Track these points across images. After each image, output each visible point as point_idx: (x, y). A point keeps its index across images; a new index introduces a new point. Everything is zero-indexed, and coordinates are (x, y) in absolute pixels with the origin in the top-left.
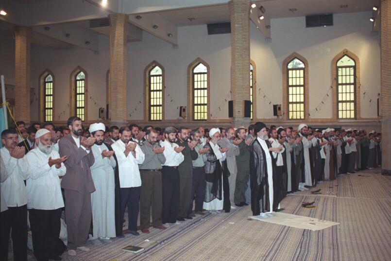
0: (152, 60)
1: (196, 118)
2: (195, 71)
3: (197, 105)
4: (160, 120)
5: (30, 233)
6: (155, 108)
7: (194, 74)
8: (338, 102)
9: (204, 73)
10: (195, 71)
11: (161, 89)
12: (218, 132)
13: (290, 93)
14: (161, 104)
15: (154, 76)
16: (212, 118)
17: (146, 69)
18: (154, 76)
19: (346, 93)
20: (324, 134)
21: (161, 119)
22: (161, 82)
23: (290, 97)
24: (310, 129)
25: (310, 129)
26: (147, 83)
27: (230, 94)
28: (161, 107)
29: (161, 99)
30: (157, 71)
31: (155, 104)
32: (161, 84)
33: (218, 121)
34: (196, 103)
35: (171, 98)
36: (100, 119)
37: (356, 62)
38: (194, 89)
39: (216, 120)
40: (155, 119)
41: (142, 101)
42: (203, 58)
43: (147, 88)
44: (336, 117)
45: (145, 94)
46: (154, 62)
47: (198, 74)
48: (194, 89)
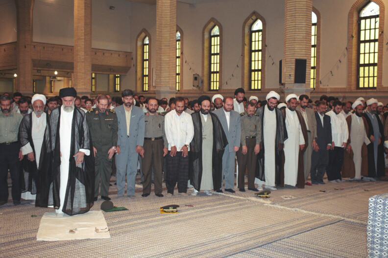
0: (251, 12)
1: (361, 86)
2: (212, 34)
3: (364, 65)
4: (258, 90)
5: (10, 189)
6: (256, 73)
7: (360, 19)
8: (359, 65)
9: (375, 17)
10: (365, 13)
11: (260, 48)
12: (360, 105)
13: (361, 52)
14: (260, 68)
15: (255, 32)
16: (321, 86)
17: (245, 23)
18: (255, 32)
19: (369, 53)
20: (356, 108)
21: (260, 88)
22: (260, 39)
23: (362, 56)
24: (305, 100)
25: (305, 100)
26: (247, 41)
27: (346, 52)
28: (260, 73)
29: (260, 62)
30: (258, 25)
31: (256, 68)
32: (260, 42)
33: (329, 90)
34: (362, 62)
35: (272, 59)
36: (195, 88)
37: (152, 40)
38: (359, 42)
39: (326, 88)
40: (256, 88)
41: (240, 65)
42: (262, 14)
43: (246, 48)
44: (353, 87)
45: (243, 55)
46: (254, 13)
47: (365, 18)
48: (359, 42)
